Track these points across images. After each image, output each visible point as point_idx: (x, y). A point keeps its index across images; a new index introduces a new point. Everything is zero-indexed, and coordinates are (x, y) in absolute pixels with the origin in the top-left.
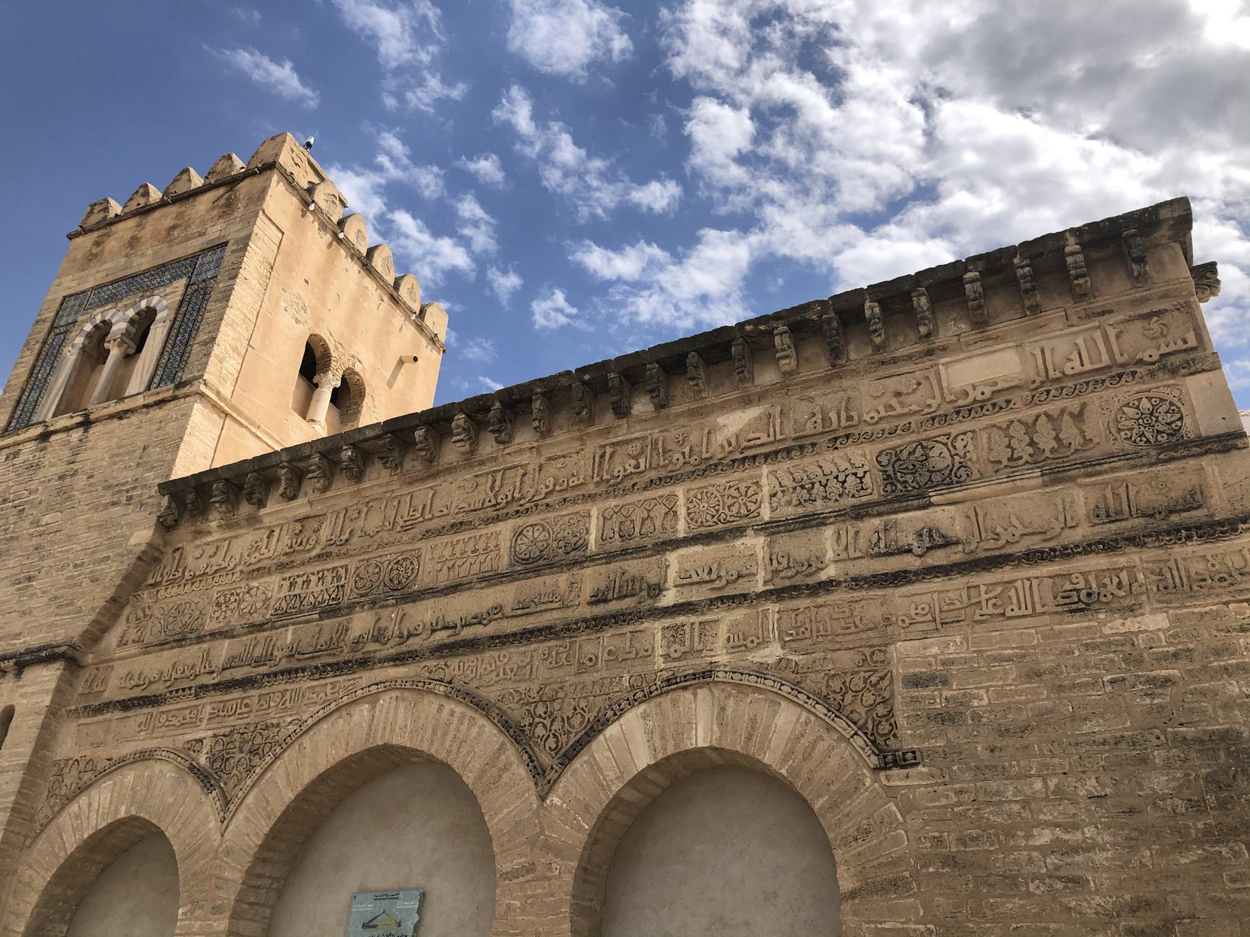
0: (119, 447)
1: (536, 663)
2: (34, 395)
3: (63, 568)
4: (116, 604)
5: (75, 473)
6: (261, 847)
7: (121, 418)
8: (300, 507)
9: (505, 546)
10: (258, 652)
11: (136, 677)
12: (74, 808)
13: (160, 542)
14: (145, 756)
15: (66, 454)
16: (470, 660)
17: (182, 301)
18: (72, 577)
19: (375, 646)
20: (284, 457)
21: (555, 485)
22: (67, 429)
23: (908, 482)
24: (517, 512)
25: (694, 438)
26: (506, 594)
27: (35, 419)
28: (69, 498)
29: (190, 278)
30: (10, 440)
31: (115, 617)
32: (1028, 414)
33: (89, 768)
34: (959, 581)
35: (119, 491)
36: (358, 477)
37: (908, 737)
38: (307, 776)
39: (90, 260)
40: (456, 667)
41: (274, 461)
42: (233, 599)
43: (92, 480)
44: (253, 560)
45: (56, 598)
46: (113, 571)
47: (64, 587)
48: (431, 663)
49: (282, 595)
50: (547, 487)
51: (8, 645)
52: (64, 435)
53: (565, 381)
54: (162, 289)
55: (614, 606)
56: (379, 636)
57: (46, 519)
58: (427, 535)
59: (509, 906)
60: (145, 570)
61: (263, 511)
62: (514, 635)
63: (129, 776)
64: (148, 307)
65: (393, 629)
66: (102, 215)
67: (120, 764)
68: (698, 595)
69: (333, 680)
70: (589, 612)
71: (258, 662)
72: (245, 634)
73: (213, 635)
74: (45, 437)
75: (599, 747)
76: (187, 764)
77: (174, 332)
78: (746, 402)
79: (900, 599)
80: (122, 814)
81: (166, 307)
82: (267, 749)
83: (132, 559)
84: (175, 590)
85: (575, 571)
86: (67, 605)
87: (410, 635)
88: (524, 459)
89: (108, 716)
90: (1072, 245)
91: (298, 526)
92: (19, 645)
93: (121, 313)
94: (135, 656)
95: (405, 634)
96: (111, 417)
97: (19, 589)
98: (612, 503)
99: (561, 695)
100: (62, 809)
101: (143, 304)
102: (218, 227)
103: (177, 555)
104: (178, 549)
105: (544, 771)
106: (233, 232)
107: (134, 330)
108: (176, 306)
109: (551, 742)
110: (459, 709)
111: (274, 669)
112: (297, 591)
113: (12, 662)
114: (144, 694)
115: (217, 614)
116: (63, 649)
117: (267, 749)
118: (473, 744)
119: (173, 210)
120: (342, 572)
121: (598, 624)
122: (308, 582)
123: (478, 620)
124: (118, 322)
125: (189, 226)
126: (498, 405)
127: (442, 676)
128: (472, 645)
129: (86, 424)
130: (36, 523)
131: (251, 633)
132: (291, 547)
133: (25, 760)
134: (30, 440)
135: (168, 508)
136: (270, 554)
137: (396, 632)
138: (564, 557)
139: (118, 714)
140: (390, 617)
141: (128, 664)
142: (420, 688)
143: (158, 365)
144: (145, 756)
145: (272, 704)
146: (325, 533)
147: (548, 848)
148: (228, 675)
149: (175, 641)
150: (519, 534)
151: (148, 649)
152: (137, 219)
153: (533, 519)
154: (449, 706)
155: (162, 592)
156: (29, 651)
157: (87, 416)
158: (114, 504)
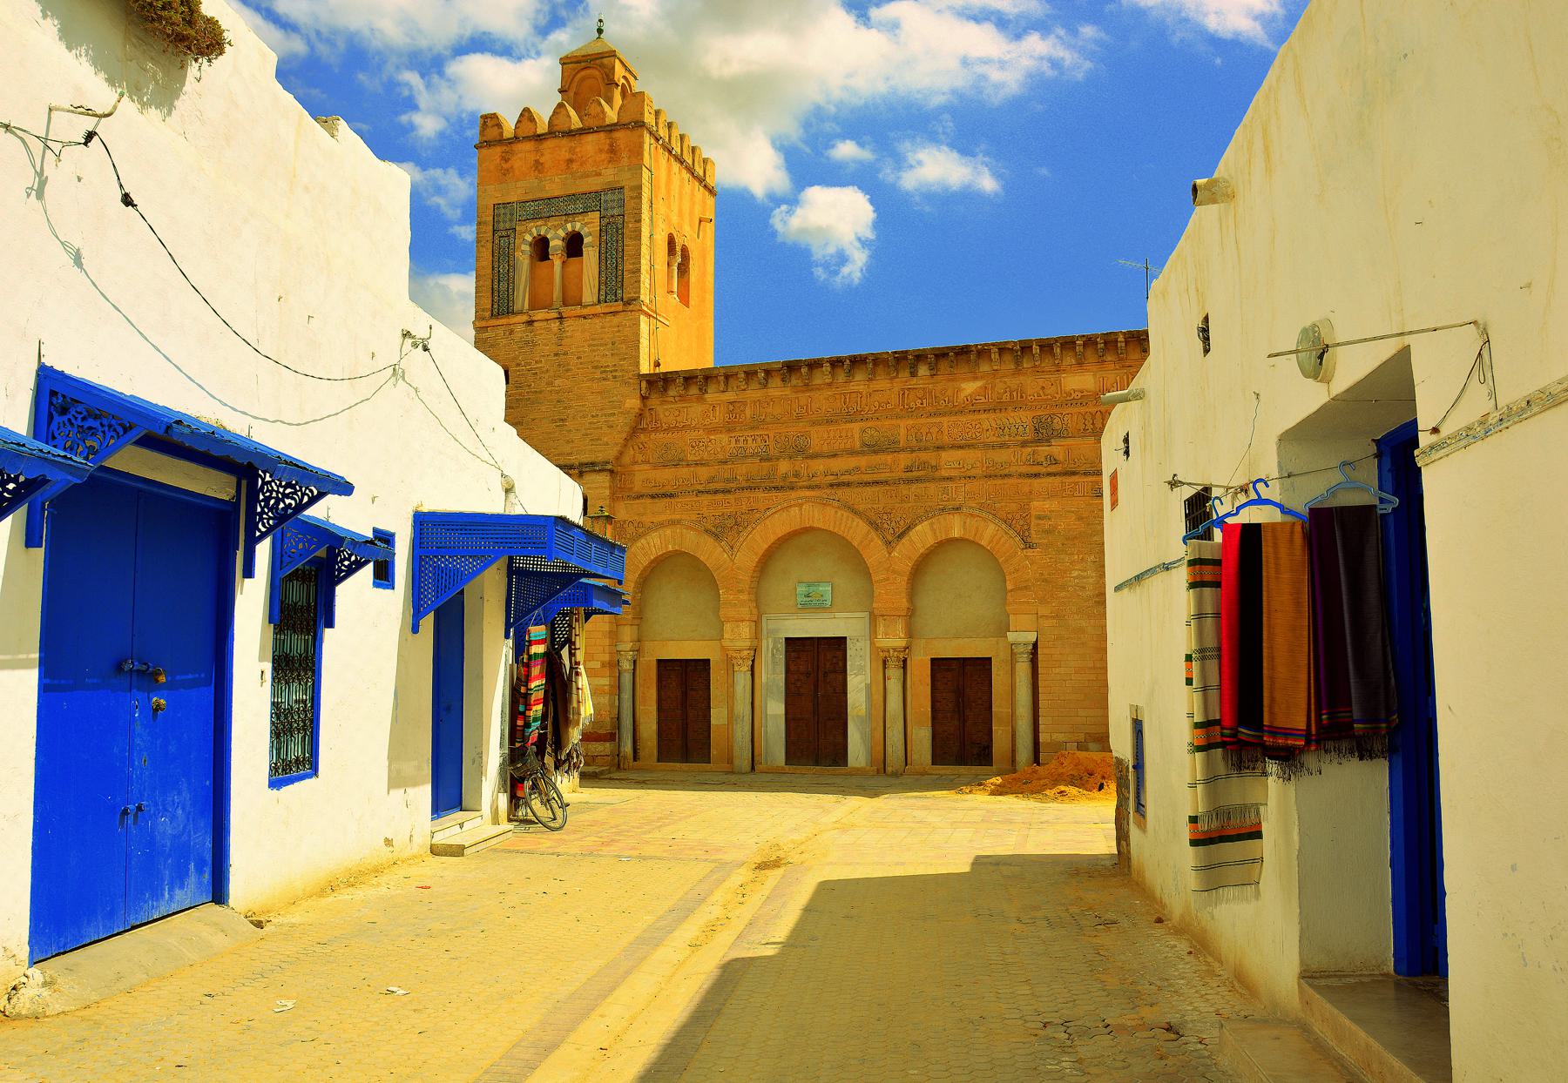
2: (503, 286)
8: (730, 396)
9: (857, 436)
14: (673, 523)
16: (847, 490)
23: (1043, 433)
25: (949, 392)
26: (862, 461)
32: (1093, 410)
34: (1058, 479)
36: (765, 386)
37: (1035, 537)
38: (772, 539)
40: (840, 493)
46: (623, 423)
55: (915, 474)
57: (557, 382)
58: (814, 423)
60: (639, 426)
65: (803, 472)
67: (661, 525)
68: (953, 473)
70: (904, 475)
71: (728, 481)
74: (530, 323)
75: (912, 533)
78: (975, 379)
79: (1036, 482)
80: (670, 548)
90: (1121, 338)
98: (911, 422)
101: (569, 226)
102: (610, 171)
106: (625, 180)
118: (856, 531)
121: (910, 481)
123: (848, 472)
128: (848, 484)
130: (550, 384)
139: (649, 501)
140: (801, 465)
141: (643, 476)
142: (824, 504)
144: (673, 523)
146: (748, 412)
147: (894, 572)
148: (712, 486)
151: (655, 467)
153: (870, 424)
156: (581, 465)
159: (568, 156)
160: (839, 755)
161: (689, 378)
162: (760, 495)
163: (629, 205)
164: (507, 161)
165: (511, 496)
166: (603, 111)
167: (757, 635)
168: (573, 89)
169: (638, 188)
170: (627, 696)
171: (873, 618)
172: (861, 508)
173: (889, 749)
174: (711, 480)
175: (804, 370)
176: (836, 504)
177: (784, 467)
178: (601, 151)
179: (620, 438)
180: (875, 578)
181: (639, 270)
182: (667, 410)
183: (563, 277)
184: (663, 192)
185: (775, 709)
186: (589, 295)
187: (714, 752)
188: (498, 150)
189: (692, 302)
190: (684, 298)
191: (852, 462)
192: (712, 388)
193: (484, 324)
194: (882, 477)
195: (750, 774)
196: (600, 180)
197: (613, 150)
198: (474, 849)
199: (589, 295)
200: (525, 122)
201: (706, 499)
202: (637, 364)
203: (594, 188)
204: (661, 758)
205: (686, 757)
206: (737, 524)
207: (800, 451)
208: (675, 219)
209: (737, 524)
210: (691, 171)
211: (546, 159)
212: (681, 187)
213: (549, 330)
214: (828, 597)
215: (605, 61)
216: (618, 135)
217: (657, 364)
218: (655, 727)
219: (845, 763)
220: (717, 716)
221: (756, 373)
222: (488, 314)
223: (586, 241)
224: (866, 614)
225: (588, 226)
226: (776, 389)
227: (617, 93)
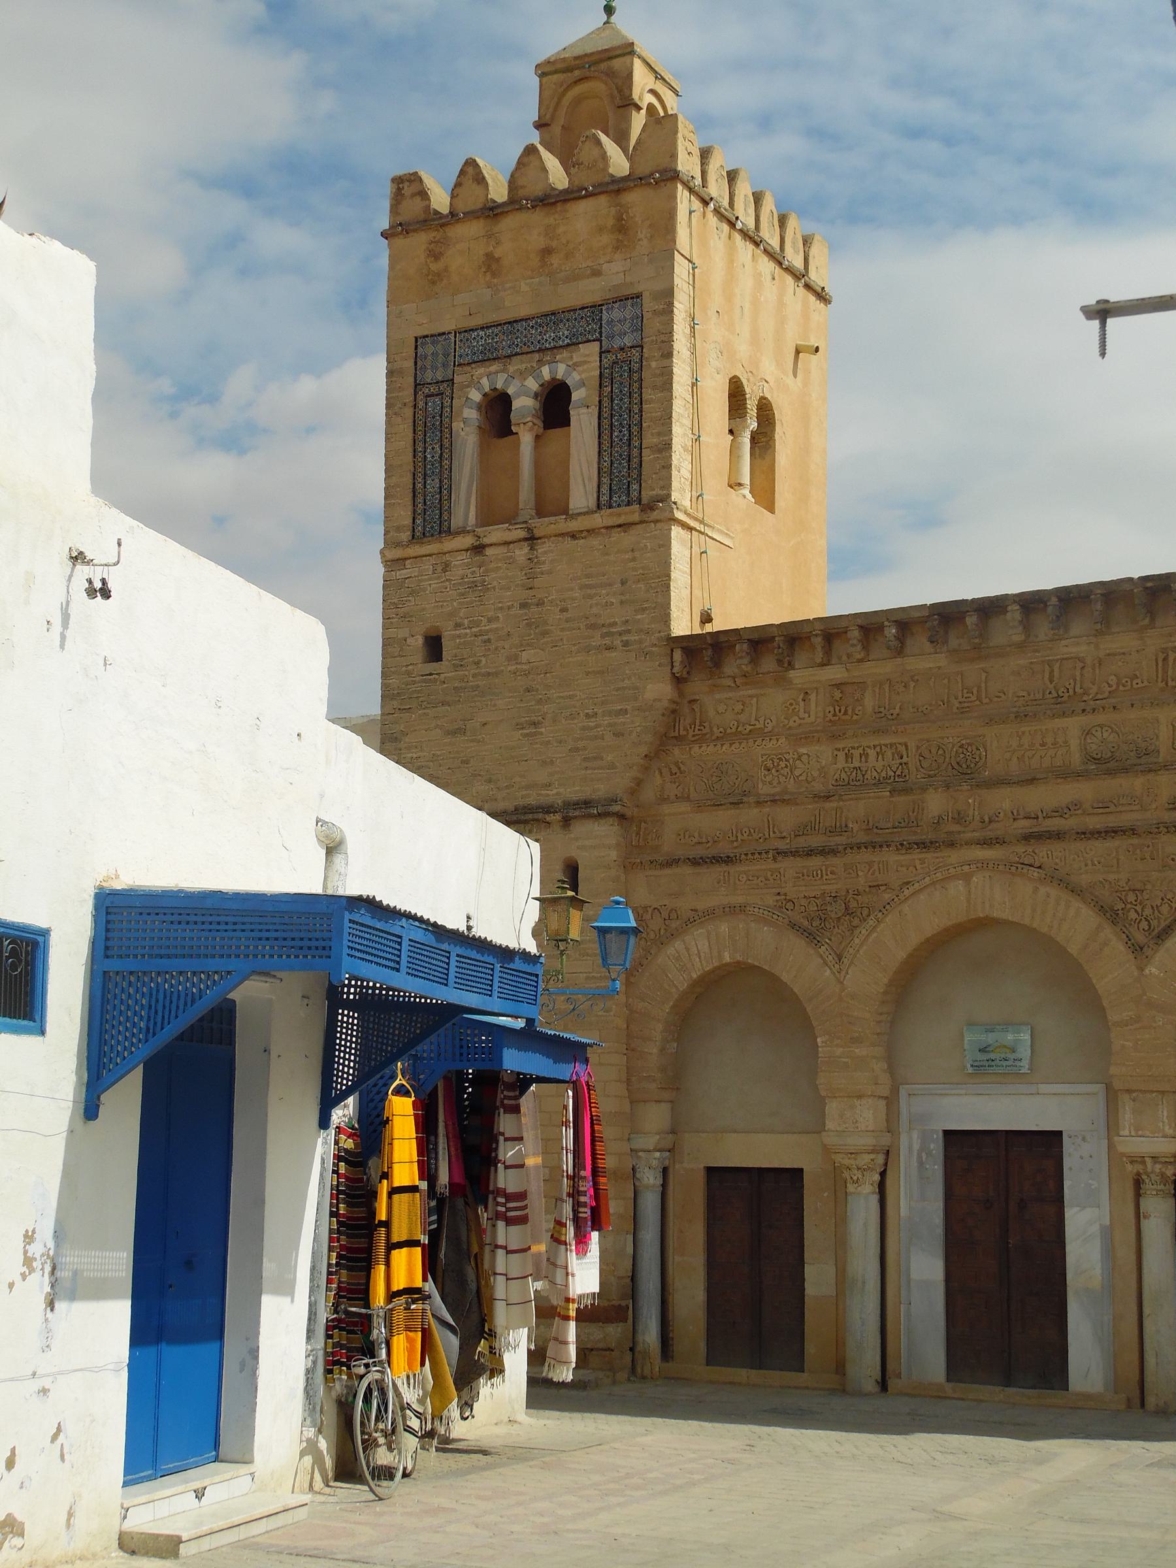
0: (588, 576)
1: (1122, 858)
3: (572, 717)
5: (540, 603)
6: (885, 993)
8: (835, 673)
9: (1074, 744)
11: (696, 835)
12: (671, 951)
14: (733, 911)
19: (956, 828)
20: (818, 626)
21: (1118, 685)
24: (1084, 711)
27: (456, 522)
28: (544, 634)
31: (647, 769)
36: (899, 651)
38: (914, 940)
39: (434, 283)
40: (1044, 852)
41: (807, 629)
42: (782, 764)
44: (791, 724)
45: (577, 750)
48: (1020, 849)
49: (839, 766)
50: (1110, 686)
51: (539, 795)
53: (1127, 587)
54: (565, 354)
56: (959, 818)
57: (525, 656)
58: (990, 722)
59: (1123, 1046)
60: (674, 729)
61: (792, 674)
62: (1099, 833)
66: (418, 203)
67: (710, 914)
69: (923, 856)
71: (832, 831)
74: (478, 549)
76: (786, 921)
77: (606, 422)
80: (727, 958)
81: (582, 384)
82: (865, 912)
85: (1151, 776)
86: (595, 758)
87: (990, 822)
88: (1082, 650)
91: (838, 694)
95: (987, 820)
96: (562, 535)
97: (527, 735)
99: (1149, 887)
101: (546, 372)
103: (696, 707)
104: (695, 701)
105: (1141, 949)
107: (538, 405)
109: (1144, 925)
110: (1054, 892)
111: (854, 840)
112: (856, 764)
113: (558, 817)
115: (768, 779)
116: (616, 808)
117: (865, 912)
118: (1076, 925)
119: (538, 218)
120: (902, 749)
122: (864, 755)
123: (1058, 812)
124: (518, 395)
125: (569, 255)
126: (1054, 600)
127: (1031, 861)
128: (1058, 836)
129: (532, 539)
130: (513, 658)
132: (835, 715)
135: (681, 662)
136: (812, 719)
137: (977, 818)
138: (1138, 761)
139: (687, 870)
144: (733, 911)
145: (860, 873)
146: (869, 702)
148: (802, 842)
150: (1088, 733)
151: (699, 807)
153: (1101, 718)
154: (1043, 890)
156: (568, 805)
157: (529, 530)
158: (608, 648)
160: (1050, 1368)
161: (759, 641)
162: (892, 857)
163: (652, 325)
164: (436, 256)
165: (338, 859)
166: (604, 156)
167: (891, 1124)
168: (561, 120)
169: (667, 296)
170: (650, 1234)
171: (1112, 1096)
172: (1085, 879)
173: (1150, 1360)
174: (801, 831)
175: (971, 620)
176: (1035, 873)
177: (935, 803)
178: (601, 230)
180: (1113, 1017)
181: (668, 446)
182: (718, 702)
183: (537, 464)
184: (717, 300)
185: (925, 1268)
186: (581, 496)
187: (810, 1349)
188: (420, 241)
189: (780, 503)
190: (765, 496)
191: (1067, 792)
192: (801, 658)
193: (398, 553)
194: (1126, 819)
195: (878, 1399)
197: (622, 227)
198: (206, 1544)
199: (581, 496)
200: (468, 182)
201: (790, 866)
202: (666, 619)
203: (588, 300)
204: (711, 1359)
205: (759, 1361)
206: (848, 912)
207: (965, 771)
208: (743, 349)
209: (848, 912)
210: (777, 258)
211: (505, 250)
212: (758, 285)
213: (511, 561)
214: (1025, 1052)
215: (617, 64)
216: (634, 198)
217: (706, 618)
218: (700, 1296)
219: (1065, 1386)
220: (817, 1279)
221: (880, 628)
222: (405, 536)
223: (575, 396)
224: (1099, 1088)
225: (580, 369)
226: (924, 659)
227: (638, 121)
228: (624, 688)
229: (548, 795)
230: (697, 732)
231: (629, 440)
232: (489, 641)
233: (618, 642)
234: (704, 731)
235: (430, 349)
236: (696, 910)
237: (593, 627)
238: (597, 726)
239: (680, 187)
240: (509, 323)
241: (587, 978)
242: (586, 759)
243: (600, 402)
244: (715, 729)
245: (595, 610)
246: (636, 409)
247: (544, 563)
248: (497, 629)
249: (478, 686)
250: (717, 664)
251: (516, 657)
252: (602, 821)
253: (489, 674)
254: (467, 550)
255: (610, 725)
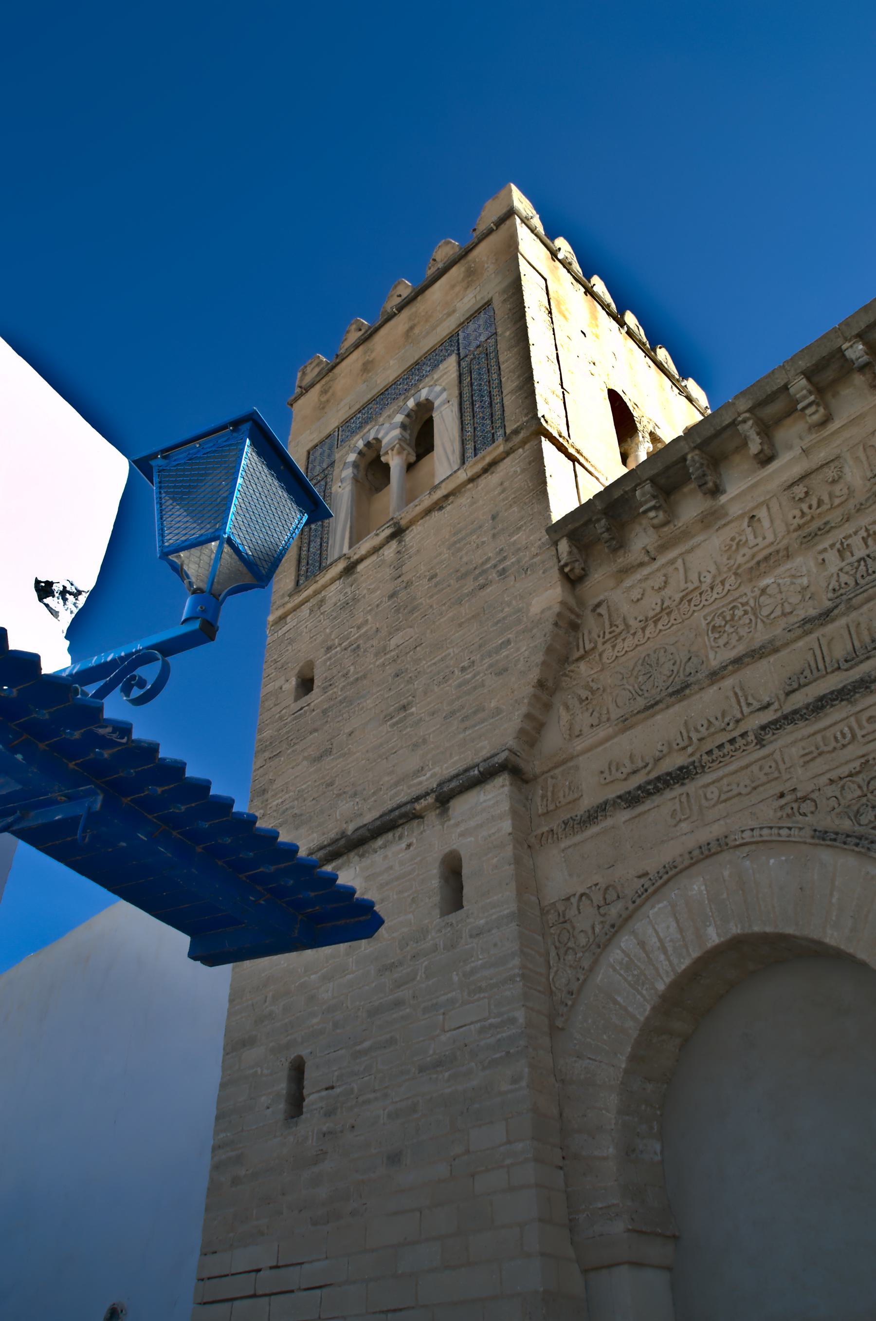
0: (455, 534)
3: (445, 679)
4: (547, 690)
5: (409, 584)
7: (441, 508)
8: (788, 465)
10: (840, 651)
11: (627, 762)
12: (615, 955)
13: (572, 602)
14: (707, 853)
15: (388, 572)
17: (460, 376)
18: (467, 682)
20: (743, 405)
22: (376, 550)
29: (459, 354)
30: (305, 594)
31: (547, 707)
33: (611, 895)
35: (484, 572)
39: (323, 408)
43: (435, 580)
45: (453, 713)
47: (458, 698)
49: (833, 569)
52: (374, 558)
54: (427, 379)
57: (393, 643)
61: (723, 499)
63: (696, 886)
64: (418, 405)
67: (671, 874)
72: (799, 638)
73: (738, 661)
74: (350, 569)
77: (467, 405)
81: (444, 390)
83: (548, 627)
84: (629, 642)
86: (475, 713)
89: (609, 822)
91: (799, 491)
92: (428, 780)
93: (387, 425)
94: (608, 739)
96: (428, 511)
97: (394, 724)
100: (595, 962)
101: (411, 403)
103: (602, 610)
107: (408, 437)
108: (456, 382)
113: (430, 799)
114: (653, 776)
115: (721, 642)
124: (387, 434)
129: (398, 533)
131: (807, 633)
132: (803, 514)
133: (513, 907)
134: (333, 581)
139: (624, 815)
143: (463, 442)
144: (707, 853)
148: (800, 699)
149: (671, 695)
152: (361, 349)
155: (609, 654)
158: (482, 587)
159: (407, 327)
178: (453, 287)
179: (522, 685)
196: (457, 315)
228: (504, 618)
229: (421, 783)
230: (607, 636)
231: (491, 404)
232: (358, 647)
233: (493, 575)
234: (618, 630)
235: (318, 454)
236: (646, 874)
237: (465, 576)
238: (474, 676)
239: (518, 221)
240: (382, 394)
241: (482, 1030)
242: (465, 718)
243: (461, 395)
244: (631, 622)
245: (465, 559)
246: (495, 376)
247: (412, 547)
248: (366, 632)
249: (345, 698)
250: (619, 544)
251: (385, 648)
252: (489, 787)
253: (357, 679)
254: (340, 578)
255: (491, 666)
